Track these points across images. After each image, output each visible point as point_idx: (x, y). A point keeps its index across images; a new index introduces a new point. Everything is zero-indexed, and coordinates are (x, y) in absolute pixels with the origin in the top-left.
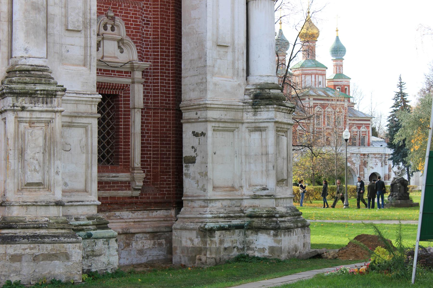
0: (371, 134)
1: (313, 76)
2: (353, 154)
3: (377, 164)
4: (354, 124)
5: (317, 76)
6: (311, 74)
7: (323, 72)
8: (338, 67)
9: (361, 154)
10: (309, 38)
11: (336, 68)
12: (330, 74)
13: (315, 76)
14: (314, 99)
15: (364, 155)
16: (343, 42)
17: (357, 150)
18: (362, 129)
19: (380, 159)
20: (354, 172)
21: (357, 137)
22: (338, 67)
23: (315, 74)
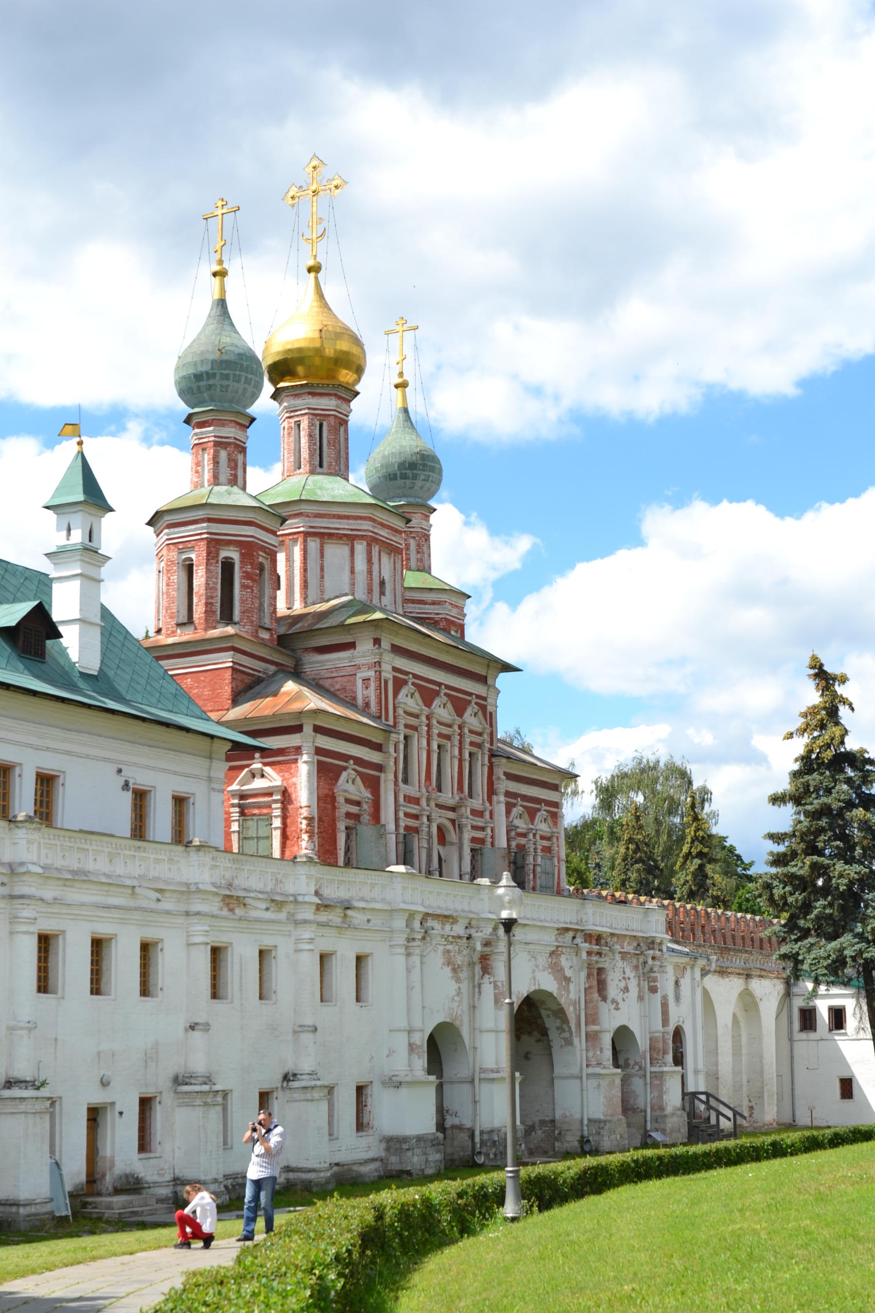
1: (360, 548)
5: (375, 549)
6: (350, 539)
13: (369, 545)
15: (597, 939)
20: (565, 1020)
22: (413, 543)
23: (372, 541)
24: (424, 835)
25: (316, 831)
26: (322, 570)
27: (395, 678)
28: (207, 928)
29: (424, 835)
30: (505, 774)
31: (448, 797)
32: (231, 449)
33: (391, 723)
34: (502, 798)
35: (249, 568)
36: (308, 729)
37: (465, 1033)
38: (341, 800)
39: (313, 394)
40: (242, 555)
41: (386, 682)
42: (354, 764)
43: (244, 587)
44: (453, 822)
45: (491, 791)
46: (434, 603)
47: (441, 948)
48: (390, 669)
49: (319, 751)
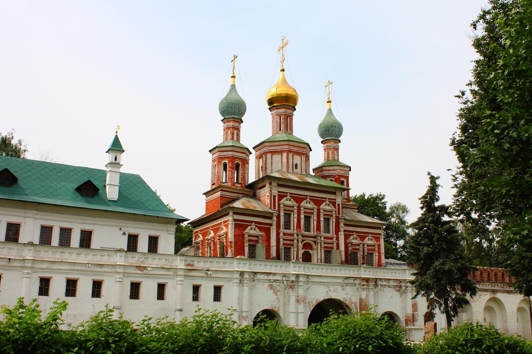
0: (383, 251)
1: (285, 155)
2: (347, 278)
4: (353, 232)
7: (301, 150)
8: (330, 152)
9: (364, 279)
10: (283, 104)
11: (328, 154)
12: (317, 158)
14: (279, 185)
16: (339, 117)
17: (356, 272)
18: (367, 241)
19: (398, 289)
20: (351, 310)
21: (360, 254)
22: (330, 152)
24: (295, 246)
25: (233, 246)
26: (272, 163)
28: (122, 276)
29: (295, 246)
30: (344, 224)
31: (312, 233)
32: (231, 129)
33: (277, 209)
34: (342, 233)
35: (231, 165)
36: (231, 213)
37: (281, 314)
38: (246, 236)
39: (277, 109)
40: (229, 161)
41: (274, 197)
43: (229, 171)
44: (315, 242)
45: (337, 230)
46: (334, 170)
48: (277, 192)
49: (235, 220)
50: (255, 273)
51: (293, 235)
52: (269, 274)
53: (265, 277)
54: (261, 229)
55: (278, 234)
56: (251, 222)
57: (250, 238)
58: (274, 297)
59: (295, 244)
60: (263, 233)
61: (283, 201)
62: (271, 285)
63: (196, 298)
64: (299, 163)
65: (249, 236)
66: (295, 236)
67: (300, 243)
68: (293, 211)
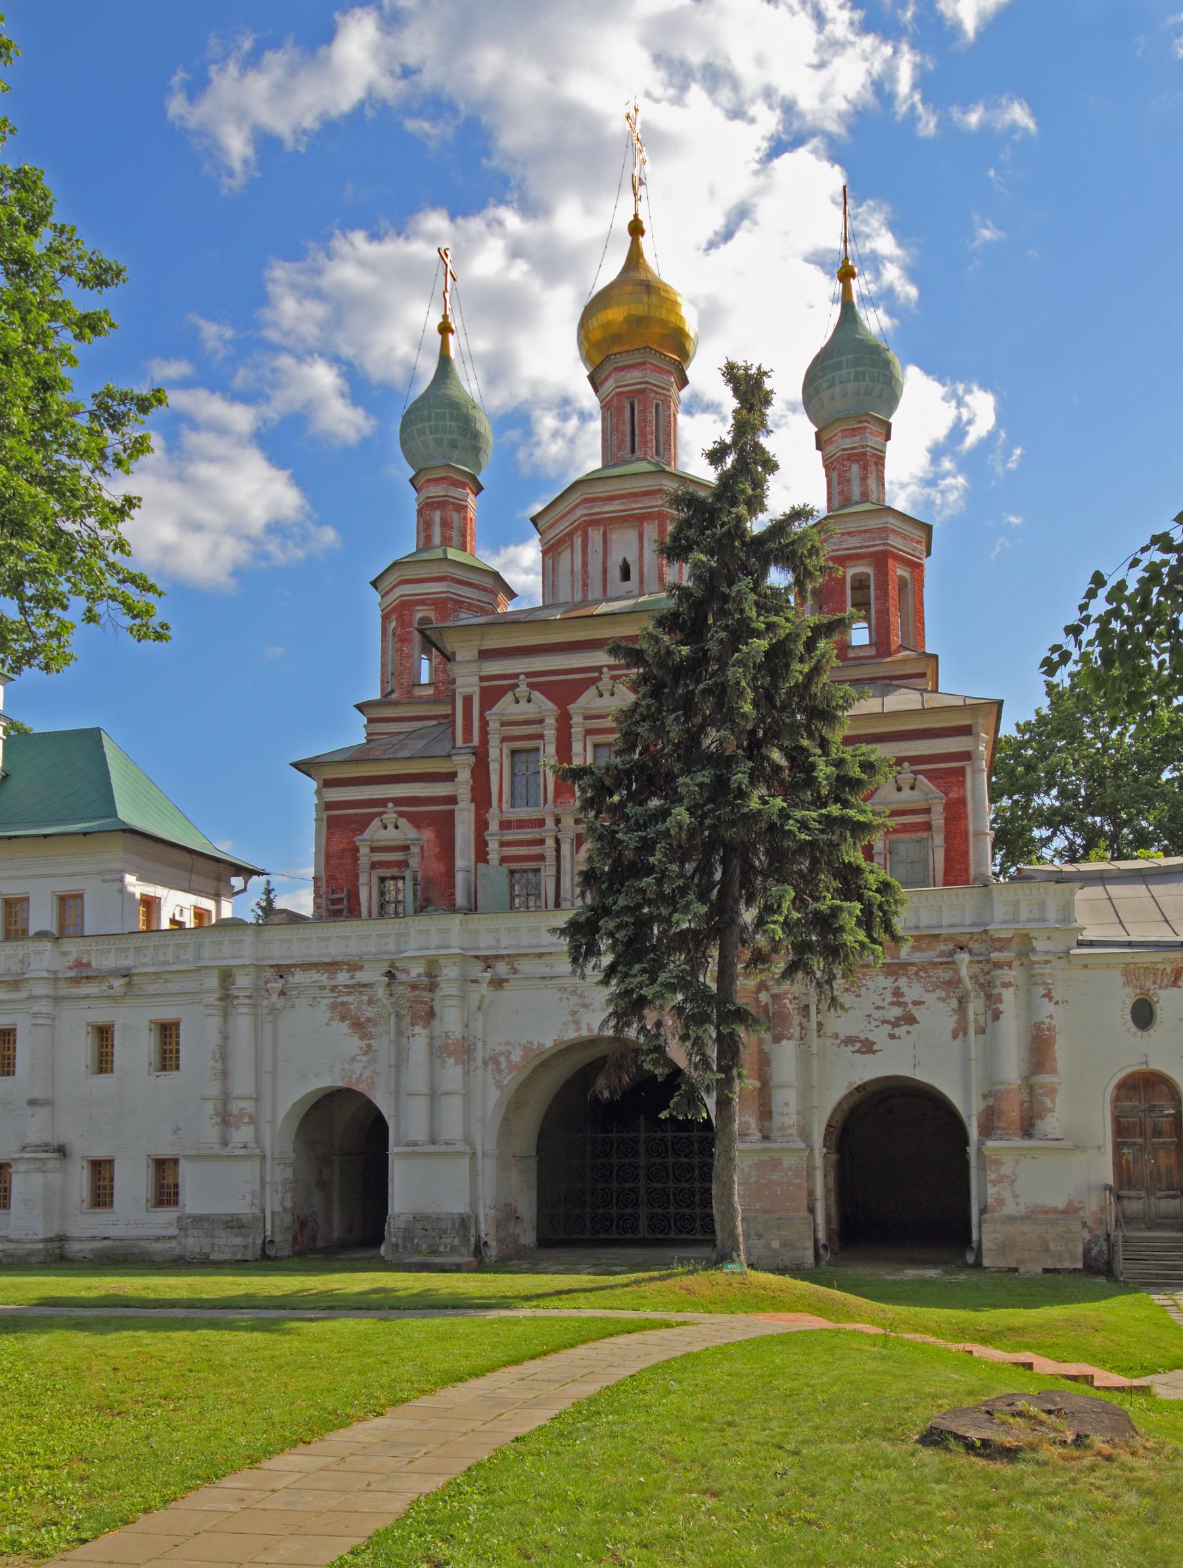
3: (910, 1020)
27: (483, 690)
38: (364, 850)
41: (468, 700)
42: (395, 805)
47: (325, 1003)
50: (282, 971)
51: (540, 823)
52: (333, 966)
53: (323, 978)
54: (416, 821)
55: (481, 825)
56: (382, 802)
57: (378, 857)
58: (355, 1044)
59: (550, 854)
60: (428, 835)
61: (506, 707)
62: (343, 1004)
63: (104, 1063)
64: (632, 559)
65: (374, 849)
66: (550, 823)
67: (566, 849)
68: (541, 737)
